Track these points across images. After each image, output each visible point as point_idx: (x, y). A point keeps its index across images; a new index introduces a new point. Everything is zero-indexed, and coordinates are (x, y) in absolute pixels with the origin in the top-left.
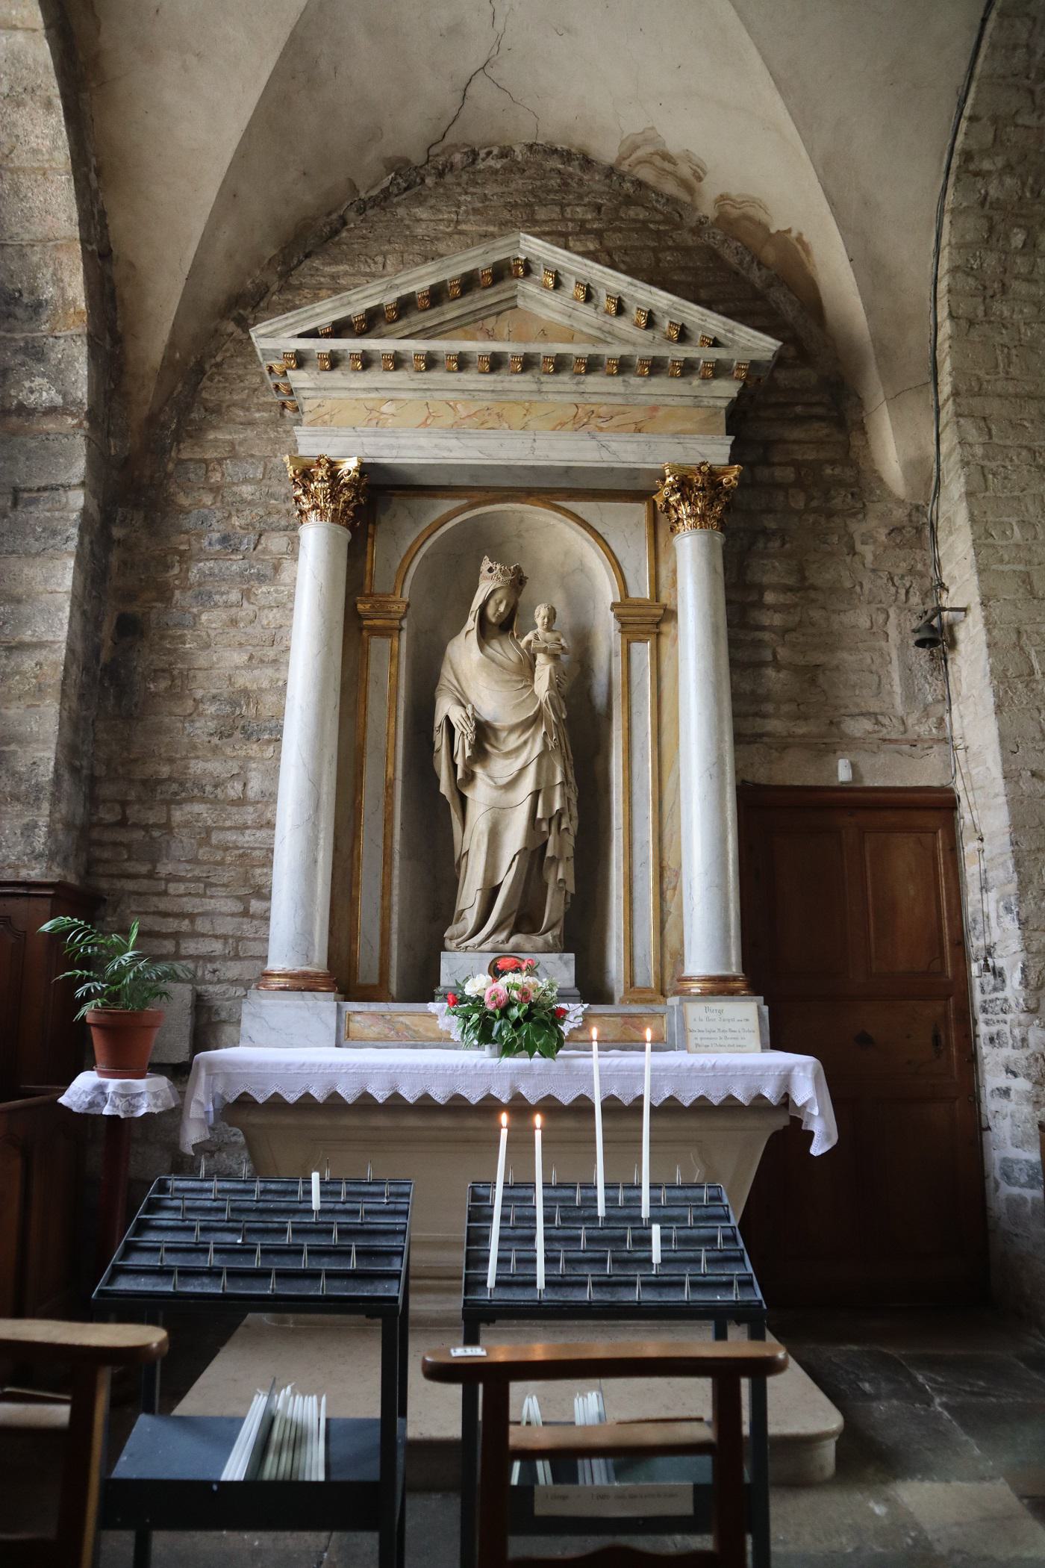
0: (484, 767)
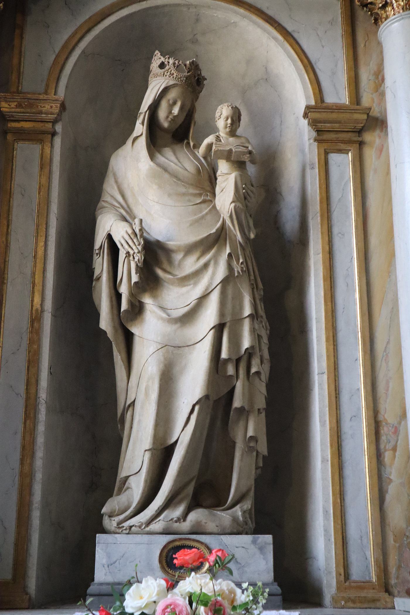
0: (155, 297)
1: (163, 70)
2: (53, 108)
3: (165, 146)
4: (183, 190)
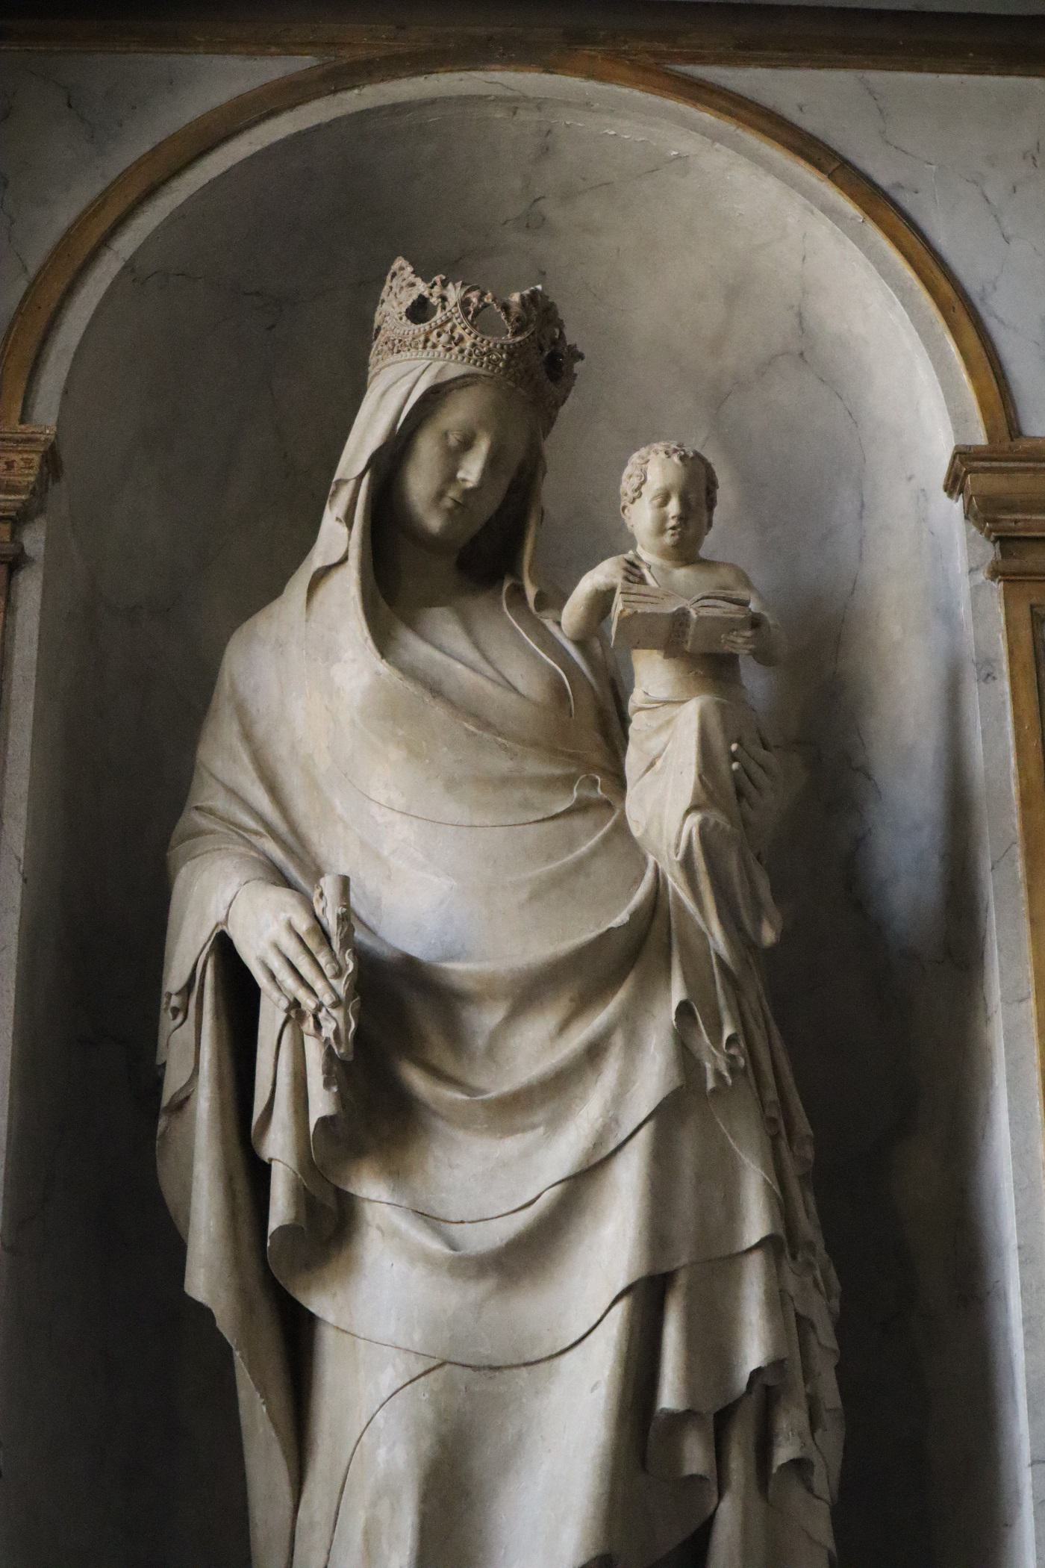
0: (397, 1173)
1: (425, 326)
2: (15, 470)
3: (432, 602)
4: (502, 764)
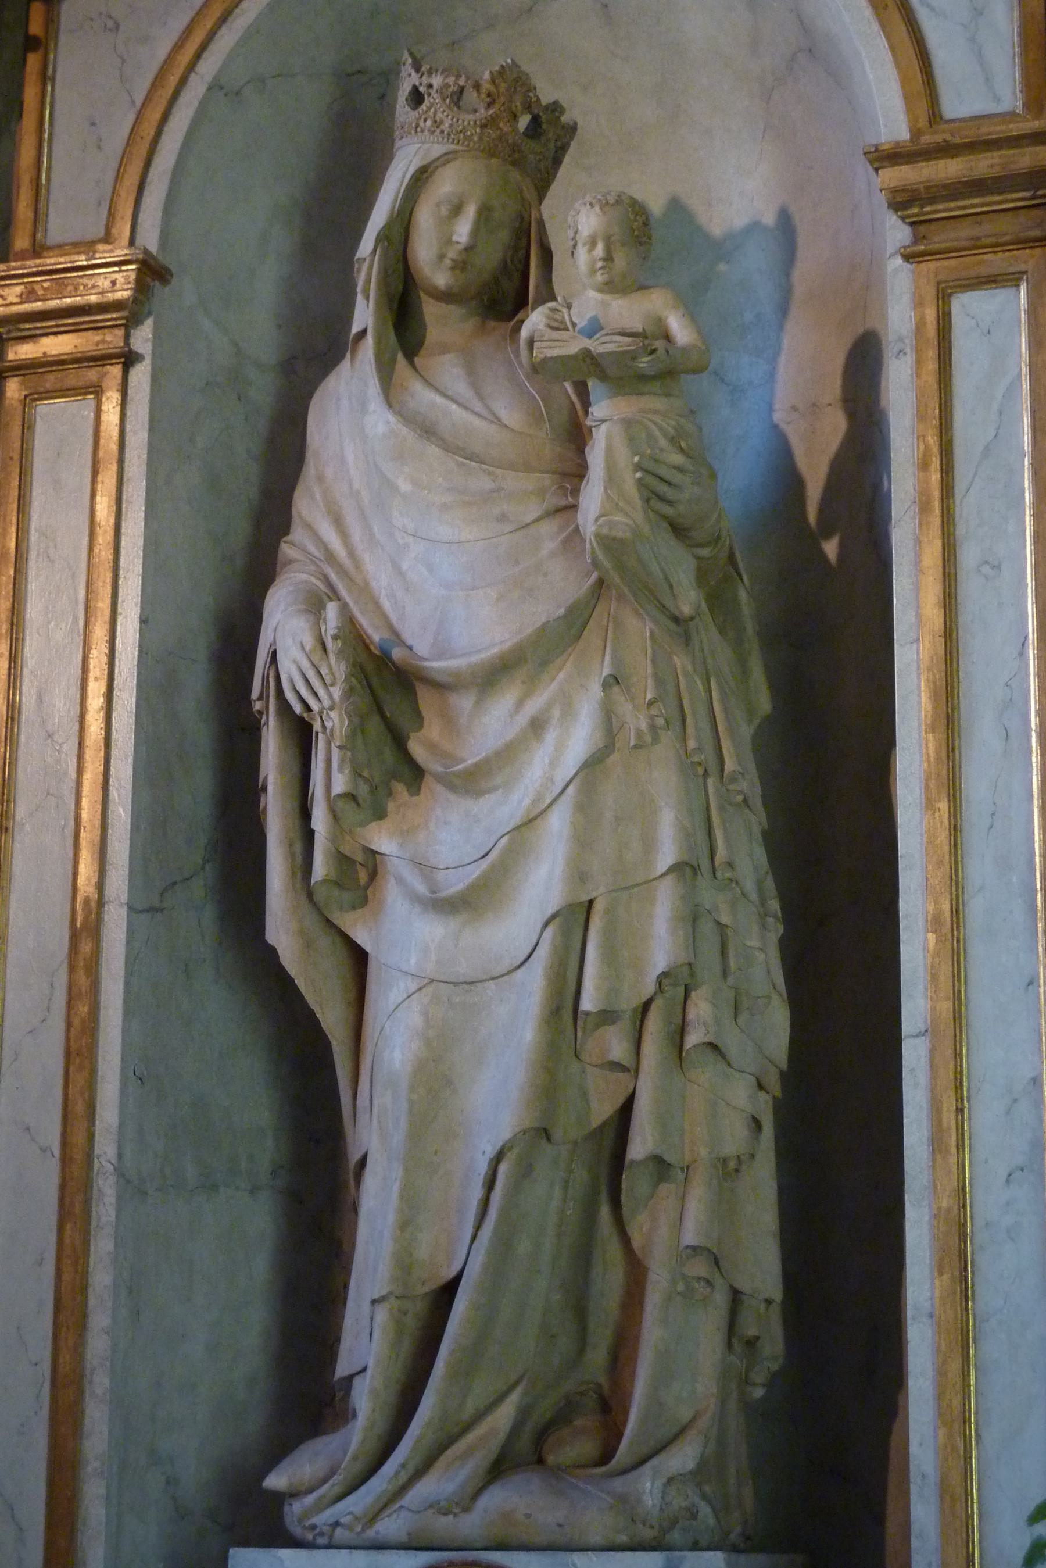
1: (416, 113)
2: (118, 286)
4: (486, 484)
